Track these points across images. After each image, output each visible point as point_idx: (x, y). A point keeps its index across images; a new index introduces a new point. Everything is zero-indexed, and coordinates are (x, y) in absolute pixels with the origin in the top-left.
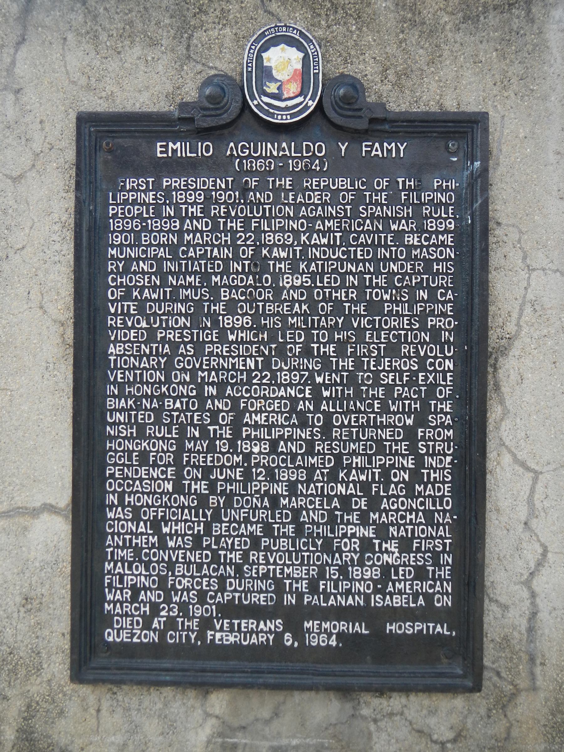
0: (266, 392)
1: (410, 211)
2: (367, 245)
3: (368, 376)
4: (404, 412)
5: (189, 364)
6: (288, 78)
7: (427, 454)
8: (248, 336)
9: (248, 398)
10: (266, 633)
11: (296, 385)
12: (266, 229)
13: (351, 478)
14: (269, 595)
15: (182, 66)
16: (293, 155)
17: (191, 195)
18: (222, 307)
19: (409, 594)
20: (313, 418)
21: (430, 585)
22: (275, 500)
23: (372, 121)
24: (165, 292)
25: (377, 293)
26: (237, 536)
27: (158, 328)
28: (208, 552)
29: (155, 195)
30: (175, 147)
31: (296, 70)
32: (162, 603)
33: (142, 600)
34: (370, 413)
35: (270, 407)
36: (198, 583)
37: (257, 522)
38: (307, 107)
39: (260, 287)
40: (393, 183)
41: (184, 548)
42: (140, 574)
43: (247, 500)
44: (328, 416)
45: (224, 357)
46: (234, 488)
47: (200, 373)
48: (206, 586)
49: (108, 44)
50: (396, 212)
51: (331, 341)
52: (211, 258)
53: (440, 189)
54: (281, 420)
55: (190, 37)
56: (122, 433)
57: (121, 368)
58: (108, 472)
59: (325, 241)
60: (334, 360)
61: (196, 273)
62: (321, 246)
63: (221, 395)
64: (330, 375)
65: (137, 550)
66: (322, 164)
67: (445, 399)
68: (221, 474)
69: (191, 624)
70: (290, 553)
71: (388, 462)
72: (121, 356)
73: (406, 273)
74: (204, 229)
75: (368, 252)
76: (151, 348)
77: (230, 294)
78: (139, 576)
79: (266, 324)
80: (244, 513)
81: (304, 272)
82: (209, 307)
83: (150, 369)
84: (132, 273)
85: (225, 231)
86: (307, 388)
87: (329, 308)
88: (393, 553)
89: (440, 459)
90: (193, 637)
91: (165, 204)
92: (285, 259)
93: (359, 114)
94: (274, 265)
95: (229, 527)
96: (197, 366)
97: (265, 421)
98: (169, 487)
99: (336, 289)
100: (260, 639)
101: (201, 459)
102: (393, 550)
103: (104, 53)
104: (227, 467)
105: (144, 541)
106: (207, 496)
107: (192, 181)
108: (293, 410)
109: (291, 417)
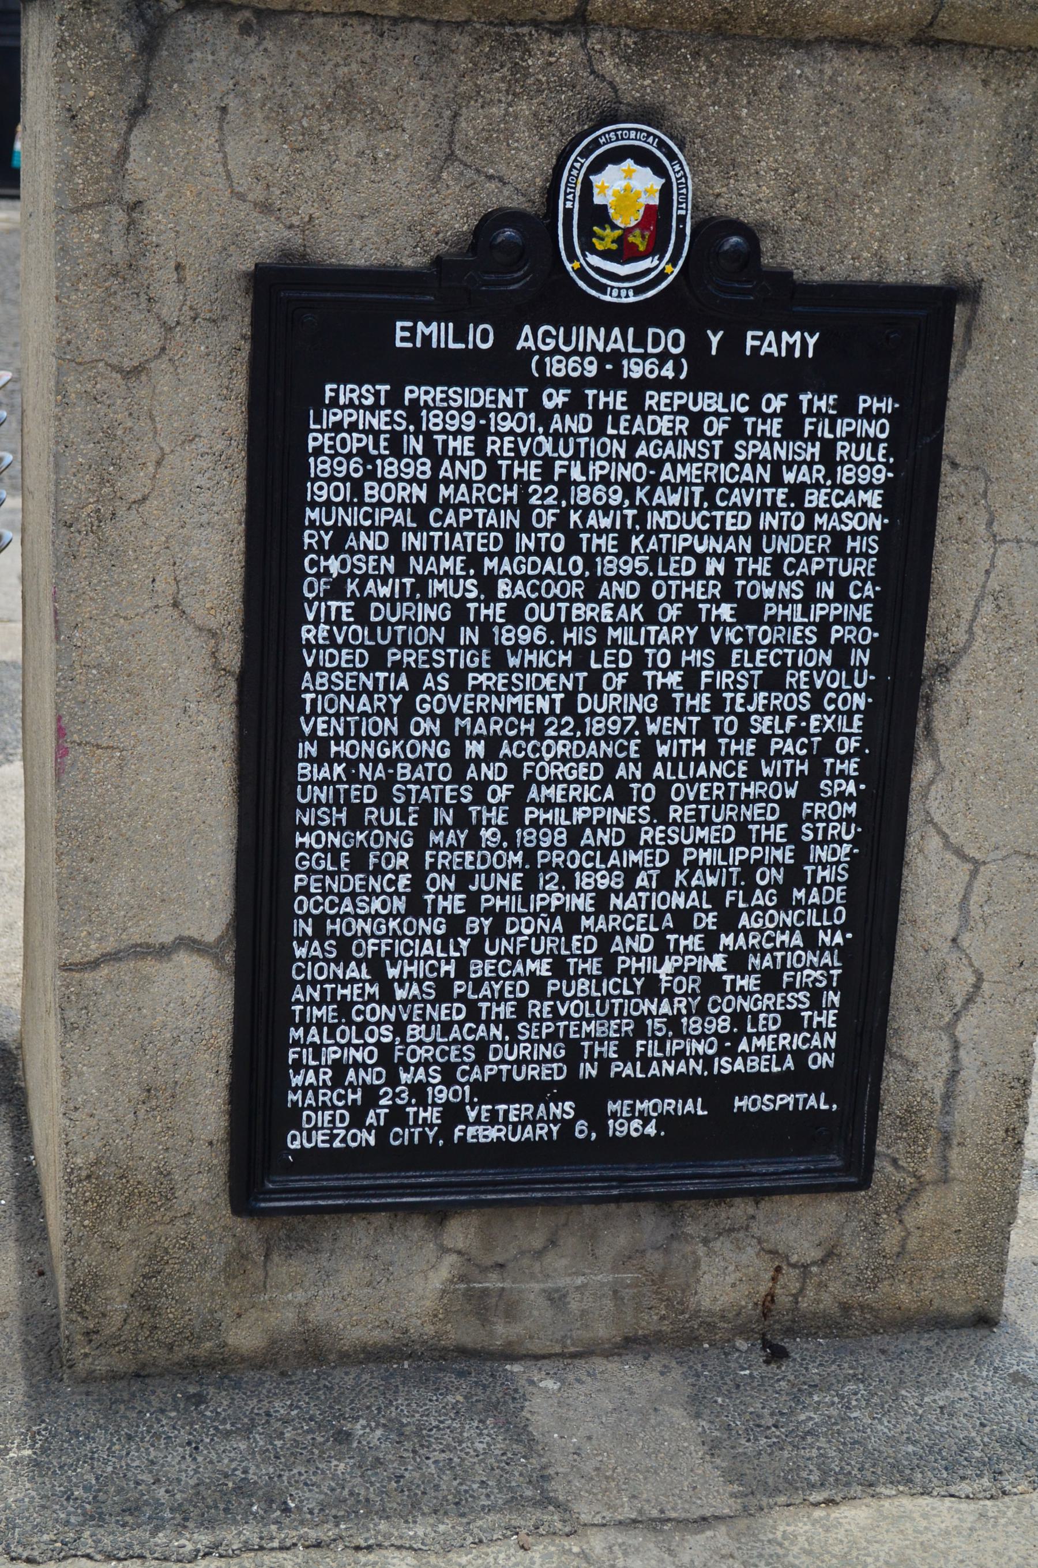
2: (743, 508)
4: (782, 779)
7: (815, 841)
9: (537, 761)
11: (615, 738)
16: (631, 350)
17: (452, 417)
22: (572, 920)
24: (403, 586)
25: (754, 588)
26: (510, 978)
30: (427, 332)
31: (648, 208)
38: (663, 276)
44: (664, 786)
45: (498, 694)
47: (457, 720)
51: (675, 666)
58: (297, 884)
59: (674, 500)
61: (457, 552)
65: (344, 1007)
66: (678, 369)
68: (488, 883)
70: (592, 1000)
72: (324, 694)
73: (803, 554)
75: (744, 518)
76: (376, 680)
85: (510, 481)
87: (673, 613)
92: (606, 531)
98: (399, 904)
99: (688, 580)
104: (496, 871)
106: (463, 917)
108: (609, 777)
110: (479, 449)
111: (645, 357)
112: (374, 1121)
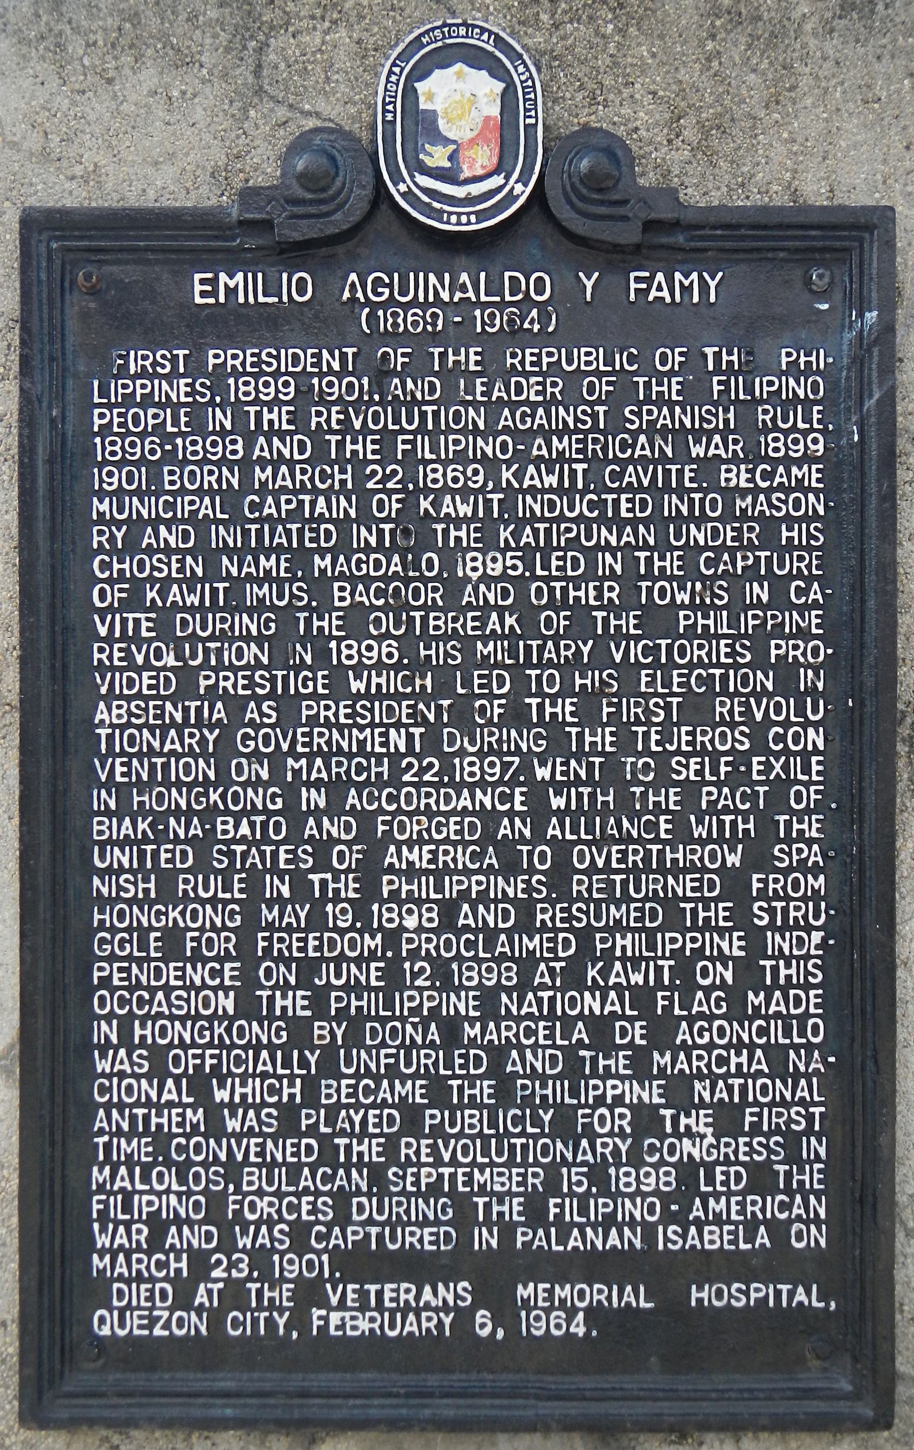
0: (432, 801)
1: (731, 416)
2: (641, 489)
3: (646, 764)
5: (267, 744)
6: (470, 135)
8: (394, 682)
9: (393, 814)
10: (436, 1310)
11: (494, 785)
12: (428, 456)
13: (612, 980)
14: (443, 1229)
15: (245, 110)
16: (484, 298)
17: (266, 385)
18: (335, 622)
19: (736, 1224)
20: (530, 853)
21: (782, 1203)
22: (451, 1029)
23: (650, 226)
24: (214, 592)
25: (662, 590)
26: (374, 1105)
27: (201, 667)
28: (313, 1142)
29: (191, 385)
30: (232, 284)
31: (487, 119)
33: (172, 1246)
34: (651, 842)
35: (439, 832)
37: (415, 1076)
38: (511, 198)
39: (415, 579)
40: (694, 358)
41: (261, 1134)
42: (168, 1191)
43: (394, 1028)
44: (562, 848)
45: (341, 728)
46: (364, 1003)
47: (290, 761)
48: (309, 1213)
49: (86, 62)
51: (566, 691)
52: (312, 519)
53: (793, 369)
54: (463, 859)
55: (262, 48)
56: (127, 891)
58: (96, 974)
59: (552, 480)
60: (574, 730)
61: (279, 550)
62: (544, 491)
63: (335, 808)
64: (566, 764)
65: (161, 1139)
66: (544, 318)
67: (808, 811)
68: (338, 976)
69: (276, 1294)
70: (485, 1139)
71: (689, 945)
72: (122, 728)
73: (724, 547)
74: (297, 457)
75: (643, 502)
76: (186, 710)
77: (352, 594)
78: (165, 1195)
80: (387, 1056)
81: (508, 547)
82: (309, 621)
83: (184, 755)
84: (144, 551)
85: (341, 461)
86: (518, 790)
88: (703, 1137)
89: (799, 938)
90: (281, 1322)
91: (212, 403)
92: (467, 520)
94: (446, 532)
95: (355, 1087)
96: (285, 747)
97: (429, 862)
98: (228, 1004)
100: (425, 1325)
101: (295, 944)
102: (702, 1129)
105: (175, 1119)
106: (309, 1021)
107: (269, 355)
108: (488, 838)
109: (484, 852)
110: (298, 419)
111: (502, 305)
112: (205, 1300)
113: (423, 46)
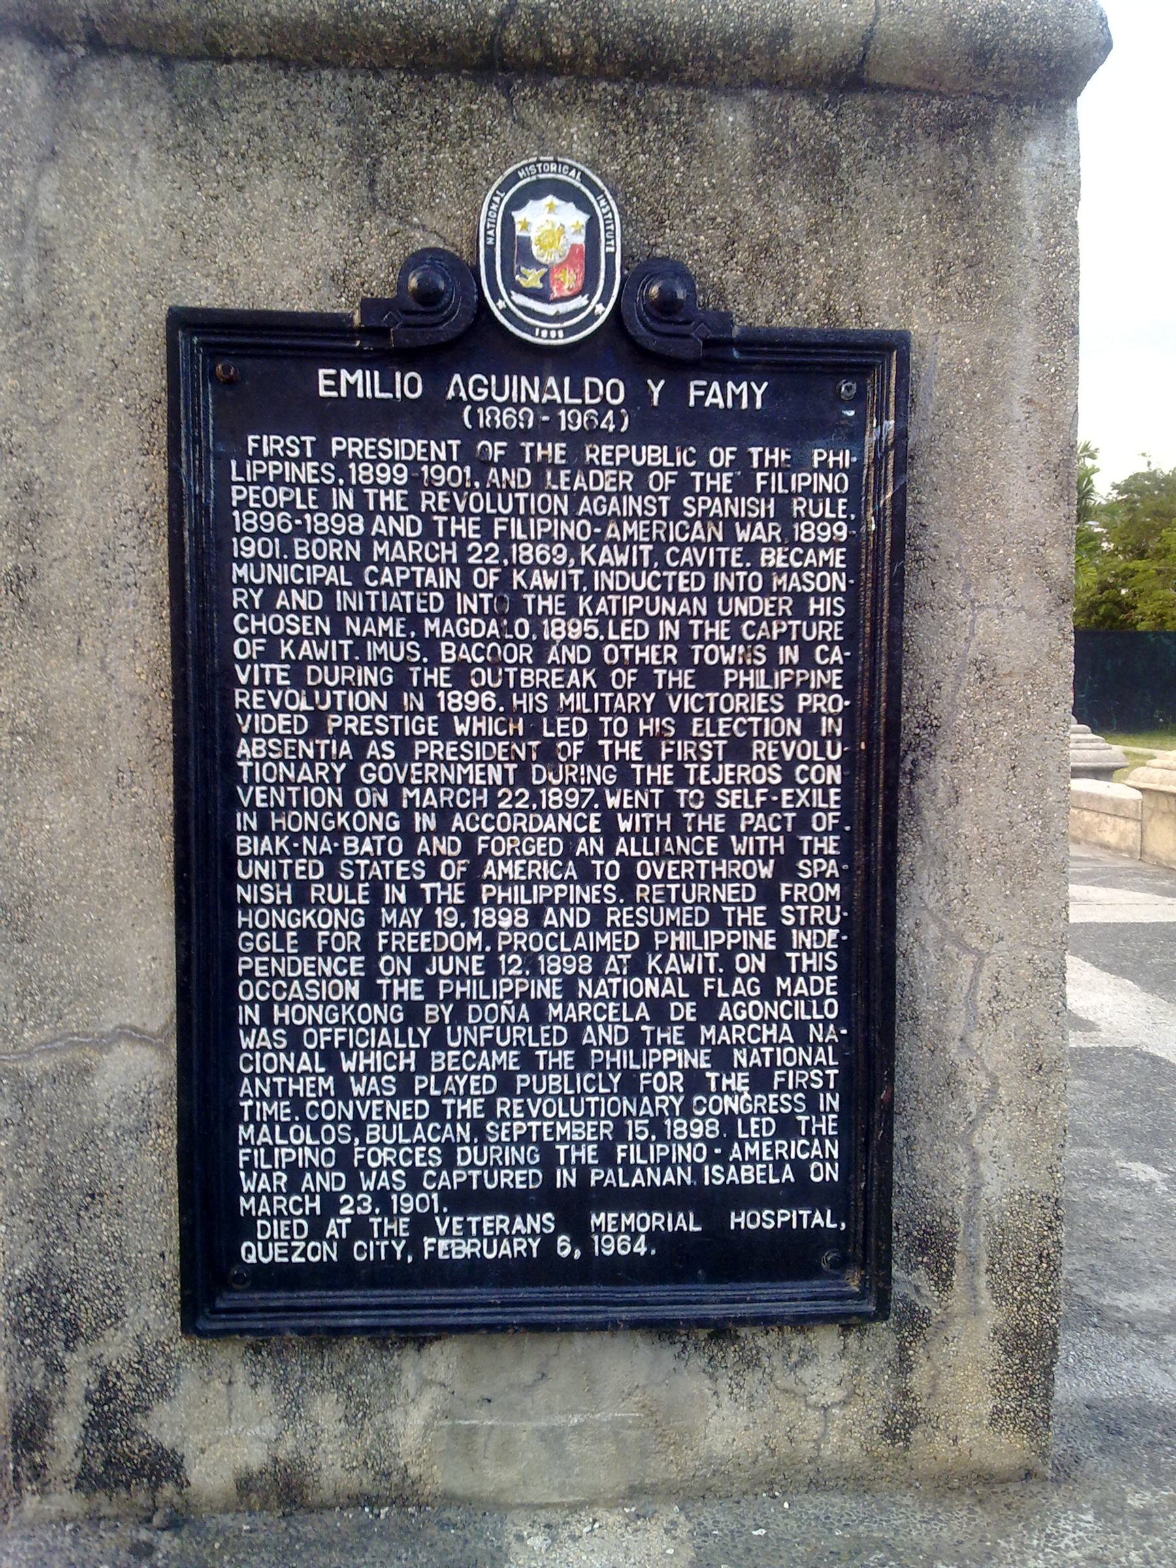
0: (523, 824)
1: (772, 506)
2: (696, 568)
3: (697, 795)
5: (386, 776)
6: (558, 261)
8: (492, 726)
9: (492, 835)
10: (526, 1236)
11: (574, 811)
12: (520, 536)
13: (668, 970)
14: (531, 1171)
15: (360, 221)
16: (568, 400)
17: (383, 470)
18: (443, 676)
19: (767, 1163)
20: (603, 867)
21: (803, 1146)
22: (538, 1009)
23: (708, 343)
24: (340, 648)
25: (712, 652)
26: (475, 1072)
27: (329, 711)
28: (425, 1102)
29: (318, 469)
30: (352, 380)
31: (574, 247)
32: (343, 1192)
33: (308, 1189)
34: (699, 857)
35: (528, 849)
36: (407, 1156)
38: (593, 317)
39: (509, 641)
40: (742, 459)
41: (382, 1097)
42: (304, 1144)
43: (492, 1009)
44: (628, 863)
45: (447, 764)
46: (468, 989)
47: (405, 791)
48: (422, 1160)
49: (219, 171)
50: (747, 509)
51: (633, 734)
52: (423, 588)
53: (823, 468)
54: (548, 871)
56: (267, 897)
57: (263, 783)
58: (241, 967)
60: (639, 767)
61: (395, 613)
62: (616, 568)
63: (443, 828)
64: (632, 794)
65: (298, 1103)
66: (618, 420)
67: (826, 832)
68: (446, 967)
69: (394, 1227)
70: (566, 1098)
71: (730, 941)
72: (262, 761)
74: (409, 534)
75: (698, 579)
77: (457, 652)
78: (302, 1147)
79: (520, 706)
80: (486, 1032)
81: (586, 615)
82: (421, 675)
83: (315, 784)
84: (277, 611)
86: (593, 816)
88: (740, 1094)
89: (819, 935)
90: (399, 1249)
91: (336, 484)
93: (685, 329)
94: (535, 602)
95: (460, 1057)
96: (401, 779)
97: (521, 873)
98: (355, 991)
100: (516, 1249)
101: (410, 941)
102: (740, 1088)
103: (212, 188)
104: (455, 954)
105: (309, 1086)
106: (421, 1004)
107: (385, 444)
109: (565, 867)
110: (412, 502)
111: (583, 407)
112: (335, 1233)
113: (519, 179)
